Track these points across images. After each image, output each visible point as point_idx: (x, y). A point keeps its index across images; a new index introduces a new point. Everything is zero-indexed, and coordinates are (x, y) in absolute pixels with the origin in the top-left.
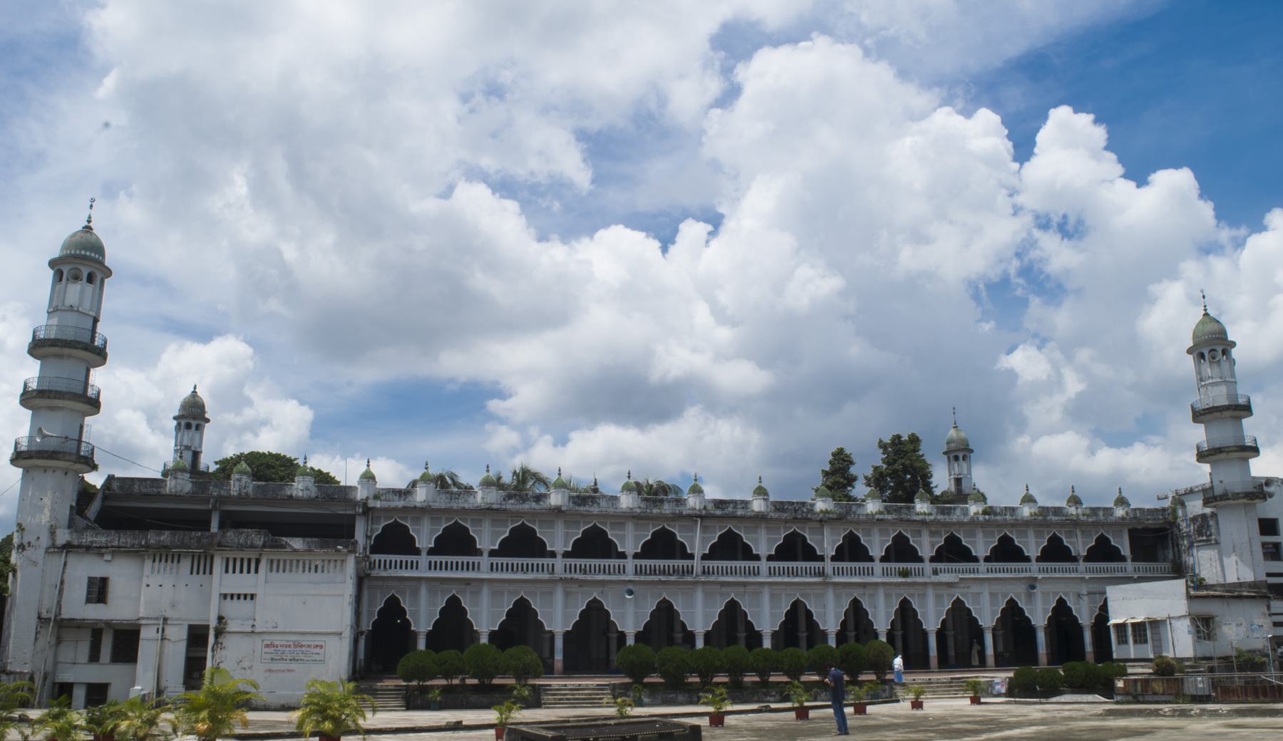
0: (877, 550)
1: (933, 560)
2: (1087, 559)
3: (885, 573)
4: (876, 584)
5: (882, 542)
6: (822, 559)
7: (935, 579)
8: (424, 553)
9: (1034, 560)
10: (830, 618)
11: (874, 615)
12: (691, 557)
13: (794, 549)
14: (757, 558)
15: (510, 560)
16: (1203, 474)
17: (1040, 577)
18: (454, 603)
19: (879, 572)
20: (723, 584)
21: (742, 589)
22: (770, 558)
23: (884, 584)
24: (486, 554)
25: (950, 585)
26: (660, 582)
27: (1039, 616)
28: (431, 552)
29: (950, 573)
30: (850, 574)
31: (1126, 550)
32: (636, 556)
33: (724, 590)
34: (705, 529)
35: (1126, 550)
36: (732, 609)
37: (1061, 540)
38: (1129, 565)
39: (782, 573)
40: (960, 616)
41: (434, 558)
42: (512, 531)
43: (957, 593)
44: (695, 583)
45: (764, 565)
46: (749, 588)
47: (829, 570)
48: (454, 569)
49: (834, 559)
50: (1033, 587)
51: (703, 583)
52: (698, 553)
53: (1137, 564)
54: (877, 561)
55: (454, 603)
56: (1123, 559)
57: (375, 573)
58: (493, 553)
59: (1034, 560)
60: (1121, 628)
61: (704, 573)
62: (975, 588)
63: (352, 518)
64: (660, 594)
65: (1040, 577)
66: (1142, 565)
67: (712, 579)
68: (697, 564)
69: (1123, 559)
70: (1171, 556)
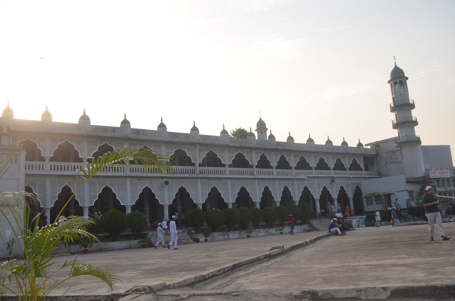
0: (274, 164)
3: (278, 174)
4: (275, 179)
7: (298, 177)
8: (47, 160)
9: (332, 169)
10: (256, 196)
12: (193, 165)
14: (224, 166)
16: (395, 133)
19: (275, 173)
21: (218, 181)
22: (230, 166)
25: (302, 180)
26: (182, 178)
27: (317, 195)
30: (263, 173)
31: (362, 166)
33: (210, 181)
34: (200, 150)
35: (362, 166)
37: (324, 160)
38: (364, 172)
39: (236, 173)
40: (306, 194)
41: (53, 163)
43: (306, 184)
44: (196, 178)
46: (222, 181)
49: (257, 167)
50: (333, 181)
51: (201, 178)
52: (197, 163)
56: (361, 170)
59: (332, 169)
60: (369, 198)
61: (200, 173)
62: (312, 181)
66: (367, 172)
67: (205, 176)
69: (361, 170)
70: (376, 169)
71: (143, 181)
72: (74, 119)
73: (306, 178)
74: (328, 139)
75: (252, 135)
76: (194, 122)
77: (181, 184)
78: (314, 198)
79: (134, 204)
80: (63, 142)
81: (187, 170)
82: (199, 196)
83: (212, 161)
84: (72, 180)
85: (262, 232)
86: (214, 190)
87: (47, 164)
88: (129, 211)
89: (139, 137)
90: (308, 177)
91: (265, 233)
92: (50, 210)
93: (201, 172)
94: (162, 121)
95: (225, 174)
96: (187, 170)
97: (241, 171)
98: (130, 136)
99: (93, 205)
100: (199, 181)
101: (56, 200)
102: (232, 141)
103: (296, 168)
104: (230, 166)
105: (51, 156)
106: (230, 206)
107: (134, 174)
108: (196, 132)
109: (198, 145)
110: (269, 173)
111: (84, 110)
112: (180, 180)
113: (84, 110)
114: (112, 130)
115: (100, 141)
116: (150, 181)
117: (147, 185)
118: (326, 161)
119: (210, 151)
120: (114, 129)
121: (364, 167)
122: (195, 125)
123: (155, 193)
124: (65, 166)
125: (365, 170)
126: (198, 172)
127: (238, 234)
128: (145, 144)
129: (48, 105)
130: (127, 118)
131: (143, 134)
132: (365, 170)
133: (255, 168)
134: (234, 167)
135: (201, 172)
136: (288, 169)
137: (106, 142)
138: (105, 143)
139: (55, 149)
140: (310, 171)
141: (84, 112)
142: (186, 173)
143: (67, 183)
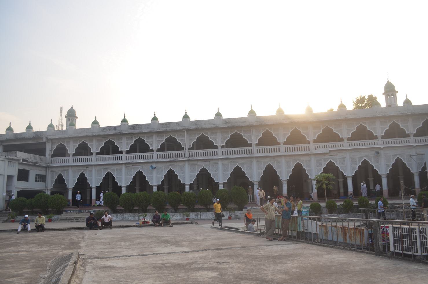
6: (250, 145)
7: (314, 152)
8: (71, 156)
18: (82, 175)
20: (198, 160)
21: (208, 163)
22: (223, 147)
23: (285, 156)
24: (94, 154)
28: (74, 155)
32: (158, 150)
33: (199, 163)
45: (220, 150)
46: (212, 162)
48: (83, 160)
51: (188, 161)
54: (282, 144)
55: (82, 175)
58: (97, 154)
63: (45, 143)
68: (187, 153)
71: (136, 166)
72: (210, 116)
73: (328, 152)
74: (341, 103)
75: (52, 127)
76: (186, 111)
77: (236, 164)
78: (345, 176)
79: (99, 186)
80: (81, 142)
81: (176, 154)
82: (124, 180)
83: (171, 145)
84: (86, 168)
85: (177, 216)
86: (109, 175)
87: (282, 147)
88: (155, 190)
89: (136, 131)
90: (330, 151)
91: (181, 217)
92: (126, 188)
94: (155, 114)
95: (217, 155)
96: (176, 154)
98: (123, 132)
99: (99, 186)
100: (187, 164)
101: (229, 177)
102: (227, 122)
104: (223, 147)
105: (73, 152)
106: (221, 187)
107: (130, 161)
108: (187, 119)
109: (186, 131)
110: (274, 150)
111: (96, 117)
112: (168, 164)
113: (96, 117)
114: (114, 129)
115: (105, 138)
116: (142, 166)
117: (139, 169)
118: (369, 128)
119: (265, 130)
120: (115, 128)
122: (52, 123)
123: (146, 176)
124: (235, 151)
126: (187, 155)
127: (150, 216)
128: (361, 122)
129: (11, 123)
130: (97, 120)
131: (137, 128)
133: (346, 140)
134: (197, 149)
137: (109, 138)
138: (109, 139)
139: (76, 147)
140: (375, 141)
141: (96, 119)
142: (175, 157)
143: (82, 171)
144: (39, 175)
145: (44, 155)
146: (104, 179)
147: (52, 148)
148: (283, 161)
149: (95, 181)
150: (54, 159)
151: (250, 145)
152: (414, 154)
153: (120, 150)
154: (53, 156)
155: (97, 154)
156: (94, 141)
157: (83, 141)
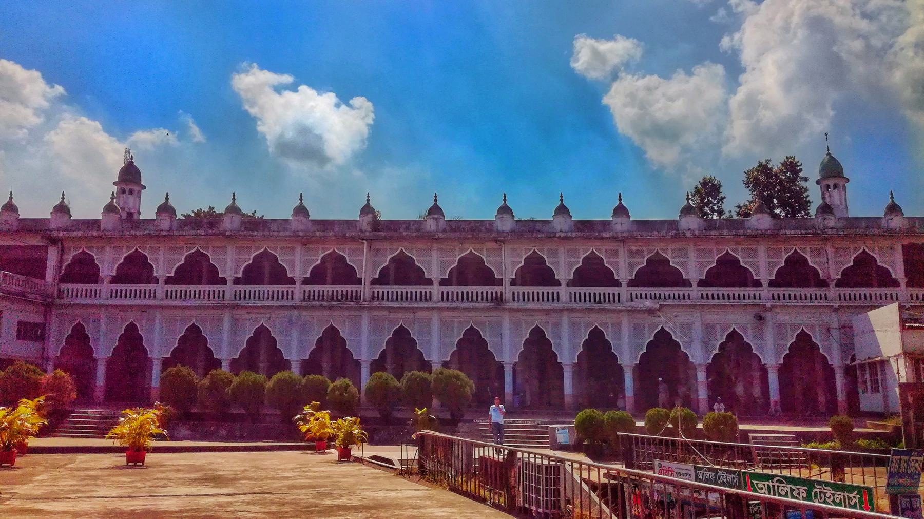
0: (563, 273)
1: (632, 284)
2: (839, 284)
3: (578, 298)
5: (570, 265)
9: (765, 284)
11: (559, 345)
13: (657, 275)
14: (429, 282)
15: (183, 287)
17: (768, 305)
25: (651, 312)
28: (114, 280)
29: (647, 298)
32: (306, 282)
33: (392, 315)
36: (401, 335)
42: (254, 258)
46: (420, 314)
47: (564, 297)
53: (915, 291)
56: (895, 284)
57: (58, 302)
58: (168, 281)
59: (765, 284)
64: (328, 321)
65: (768, 305)
69: (895, 284)
93: (376, 295)
97: (450, 294)
103: (632, 284)
116: (268, 315)
121: (906, 276)
125: (910, 284)
132: (910, 284)
135: (376, 295)
136: (744, 285)
144: (26, 324)
145: (42, 276)
146: (182, 340)
147: (61, 261)
148: (565, 319)
149: (159, 344)
150: (65, 286)
151: (500, 283)
152: (835, 325)
153: (220, 275)
154: (64, 279)
155: (168, 281)
156: (161, 251)
157: (136, 250)
